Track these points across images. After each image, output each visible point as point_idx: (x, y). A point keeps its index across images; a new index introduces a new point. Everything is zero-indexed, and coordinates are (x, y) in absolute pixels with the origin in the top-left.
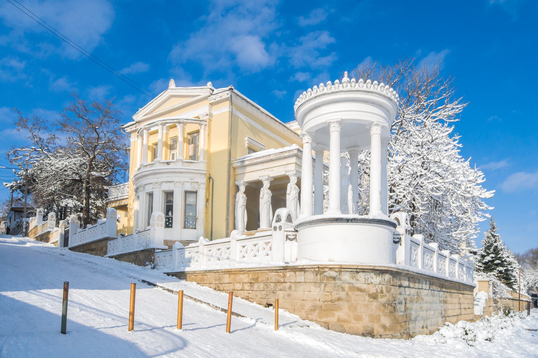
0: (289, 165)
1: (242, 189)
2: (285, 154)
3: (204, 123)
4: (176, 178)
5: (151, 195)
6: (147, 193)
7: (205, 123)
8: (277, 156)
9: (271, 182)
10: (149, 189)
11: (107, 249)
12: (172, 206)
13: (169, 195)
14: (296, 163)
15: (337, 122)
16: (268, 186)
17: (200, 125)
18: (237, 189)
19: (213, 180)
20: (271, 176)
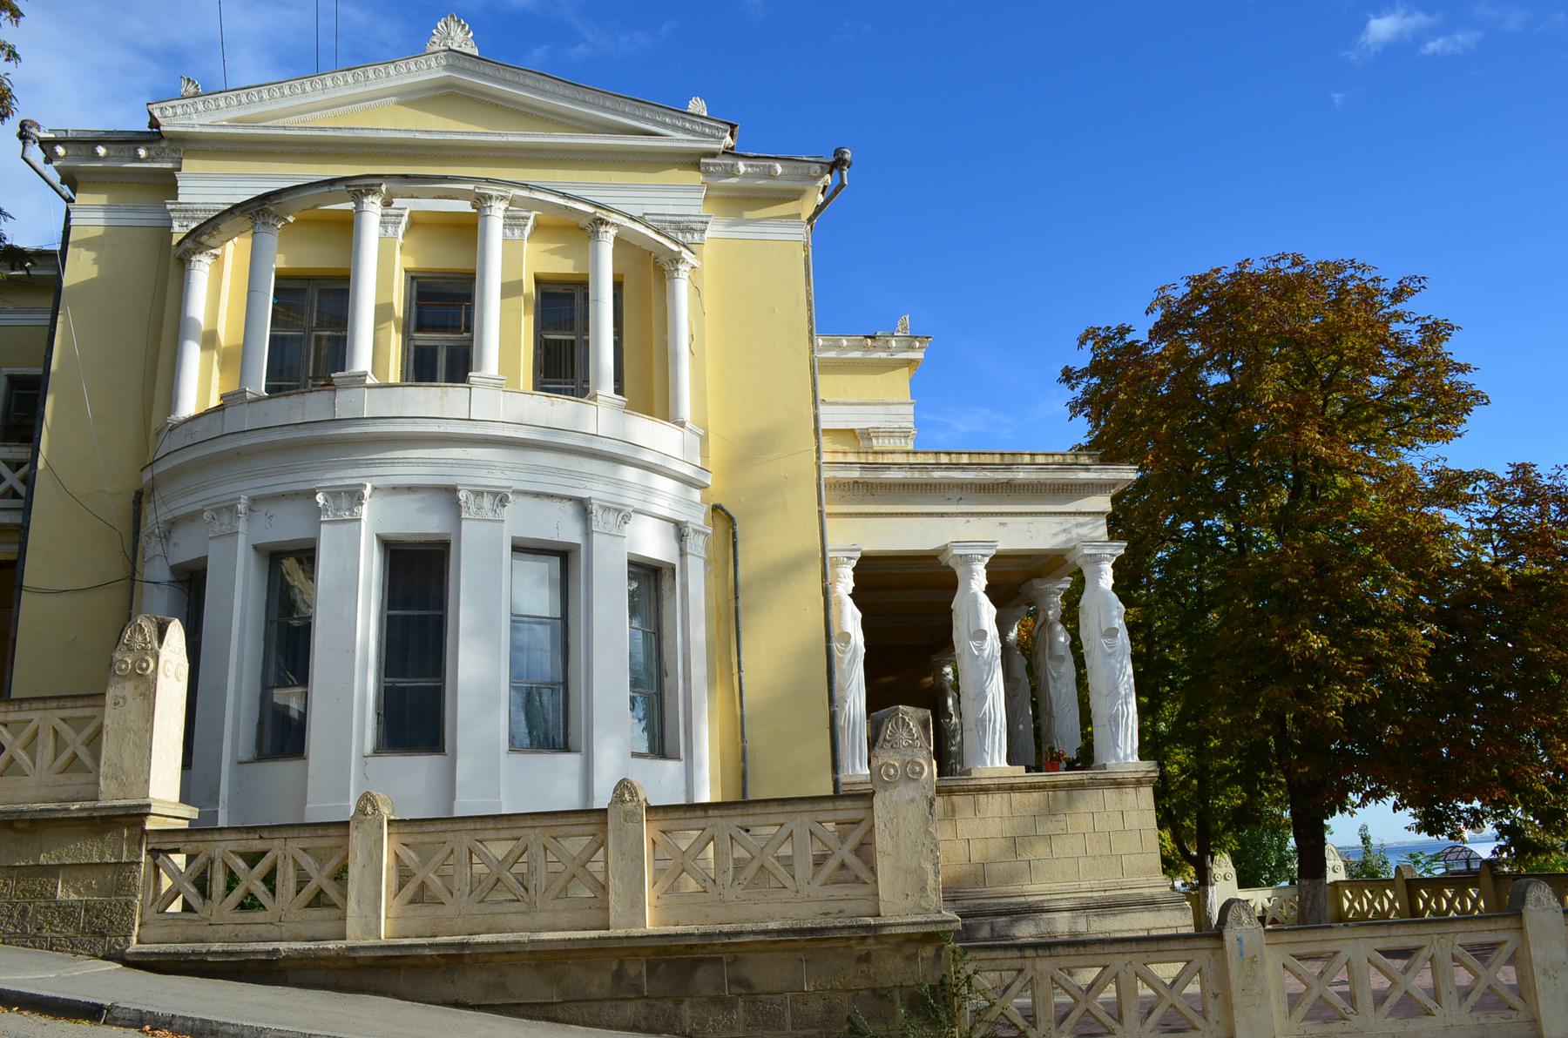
1: (845, 583)
2: (1083, 475)
19: (730, 520)
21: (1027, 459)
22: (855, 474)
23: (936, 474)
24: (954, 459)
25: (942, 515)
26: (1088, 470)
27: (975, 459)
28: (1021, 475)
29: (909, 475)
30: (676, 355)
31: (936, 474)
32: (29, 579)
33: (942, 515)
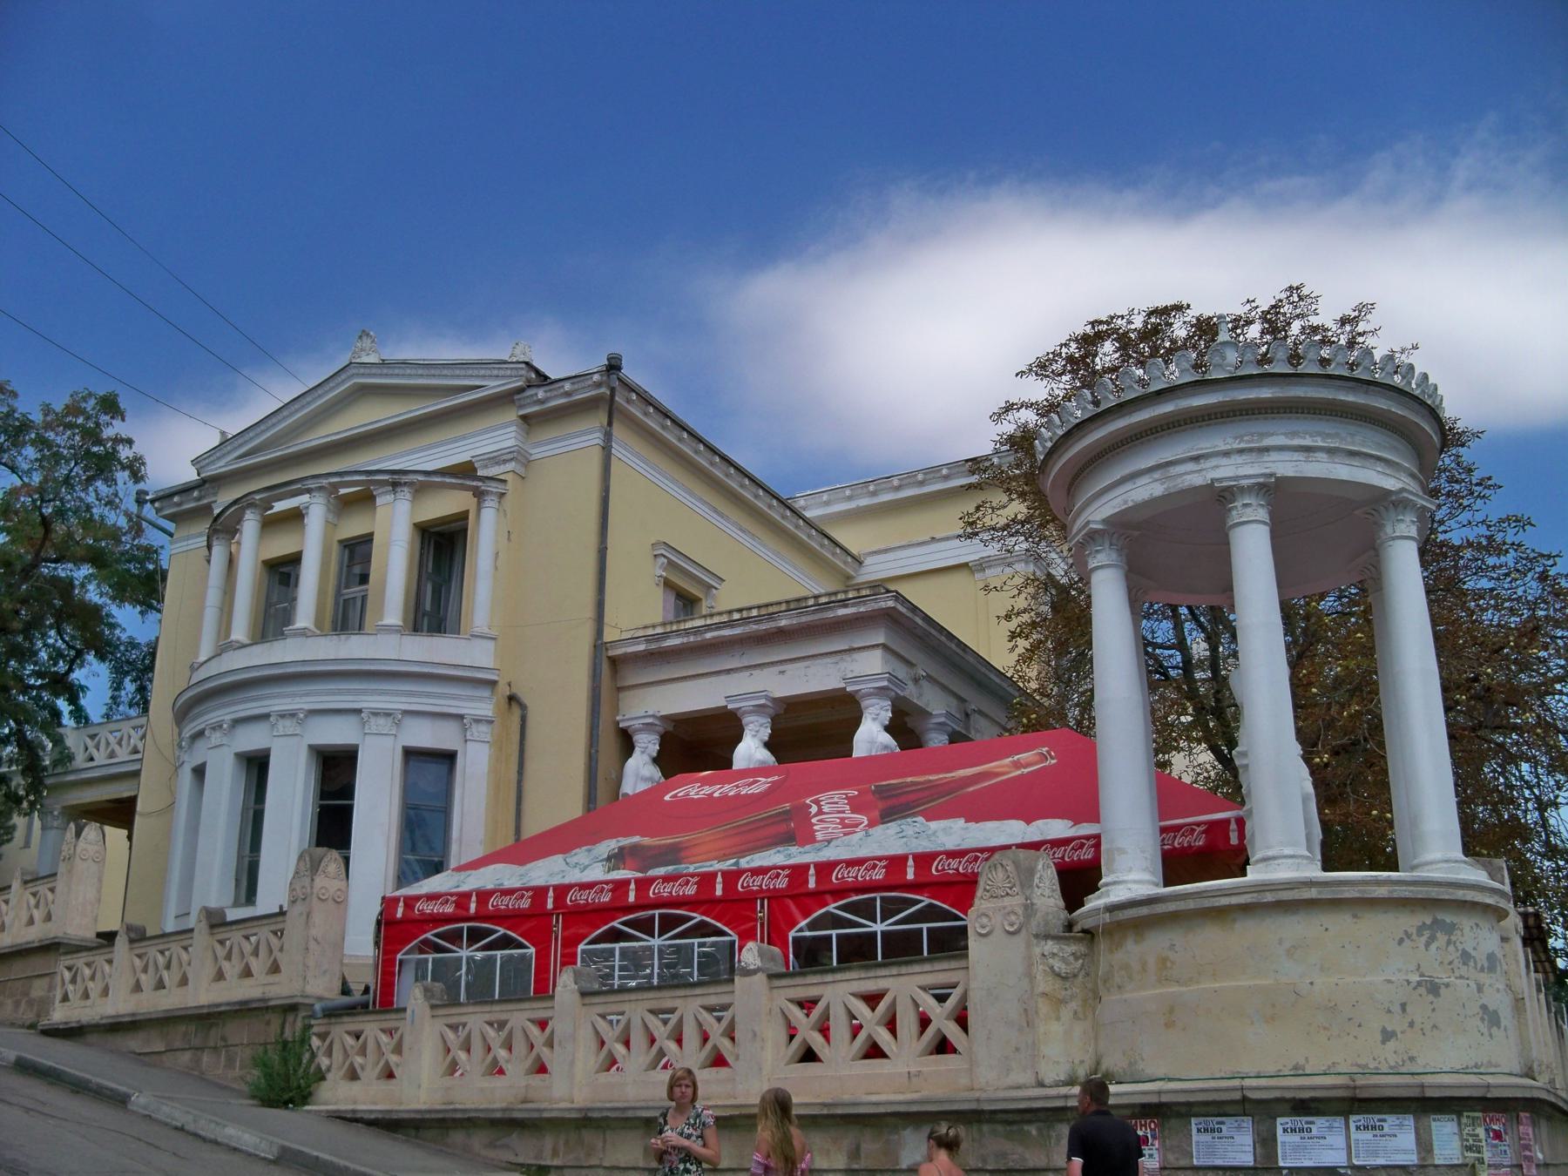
0: (856, 656)
1: (647, 744)
2: (841, 612)
3: (493, 487)
4: (371, 700)
5: (257, 766)
6: (239, 756)
7: (499, 488)
8: (804, 619)
9: (775, 721)
10: (251, 739)
11: (51, 988)
12: (348, 811)
13: (336, 769)
14: (885, 647)
15: (1261, 486)
16: (766, 733)
17: (479, 495)
18: (626, 743)
19: (523, 707)
20: (778, 695)
21: (811, 602)
22: (642, 647)
23: (709, 635)
24: (745, 614)
25: (728, 671)
26: (846, 606)
27: (763, 611)
28: (783, 623)
29: (685, 640)
30: (1130, 413)
31: (709, 635)
32: (139, 808)
33: (728, 671)
